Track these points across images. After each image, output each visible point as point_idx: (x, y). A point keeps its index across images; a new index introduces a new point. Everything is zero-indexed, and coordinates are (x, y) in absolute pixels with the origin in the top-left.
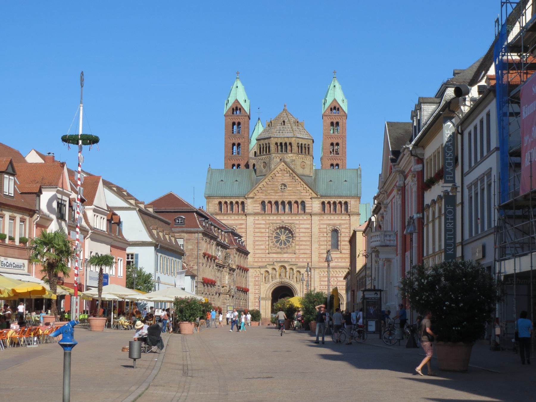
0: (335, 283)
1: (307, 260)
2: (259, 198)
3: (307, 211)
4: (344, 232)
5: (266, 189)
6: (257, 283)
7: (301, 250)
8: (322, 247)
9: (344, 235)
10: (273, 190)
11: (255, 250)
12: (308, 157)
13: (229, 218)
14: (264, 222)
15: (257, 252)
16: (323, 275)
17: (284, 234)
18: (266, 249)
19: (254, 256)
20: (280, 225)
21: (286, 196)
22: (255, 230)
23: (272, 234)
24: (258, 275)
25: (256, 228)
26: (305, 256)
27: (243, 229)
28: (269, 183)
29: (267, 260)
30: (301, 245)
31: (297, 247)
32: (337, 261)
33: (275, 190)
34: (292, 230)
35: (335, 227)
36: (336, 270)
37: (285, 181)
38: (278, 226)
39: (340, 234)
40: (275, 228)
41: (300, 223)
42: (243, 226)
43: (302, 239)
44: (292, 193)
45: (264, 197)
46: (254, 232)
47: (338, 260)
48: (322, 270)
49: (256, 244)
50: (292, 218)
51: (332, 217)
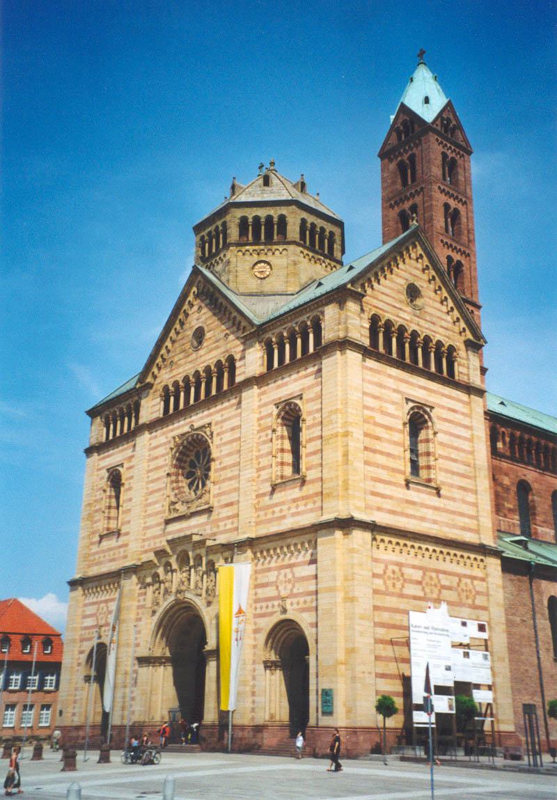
0: (290, 586)
1: (232, 523)
2: (161, 382)
4: (310, 413)
5: (173, 354)
7: (223, 498)
8: (264, 474)
12: (281, 248)
21: (201, 356)
26: (230, 514)
30: (224, 481)
35: (290, 404)
36: (289, 541)
37: (203, 318)
40: (181, 448)
41: (224, 417)
43: (228, 461)
45: (167, 376)
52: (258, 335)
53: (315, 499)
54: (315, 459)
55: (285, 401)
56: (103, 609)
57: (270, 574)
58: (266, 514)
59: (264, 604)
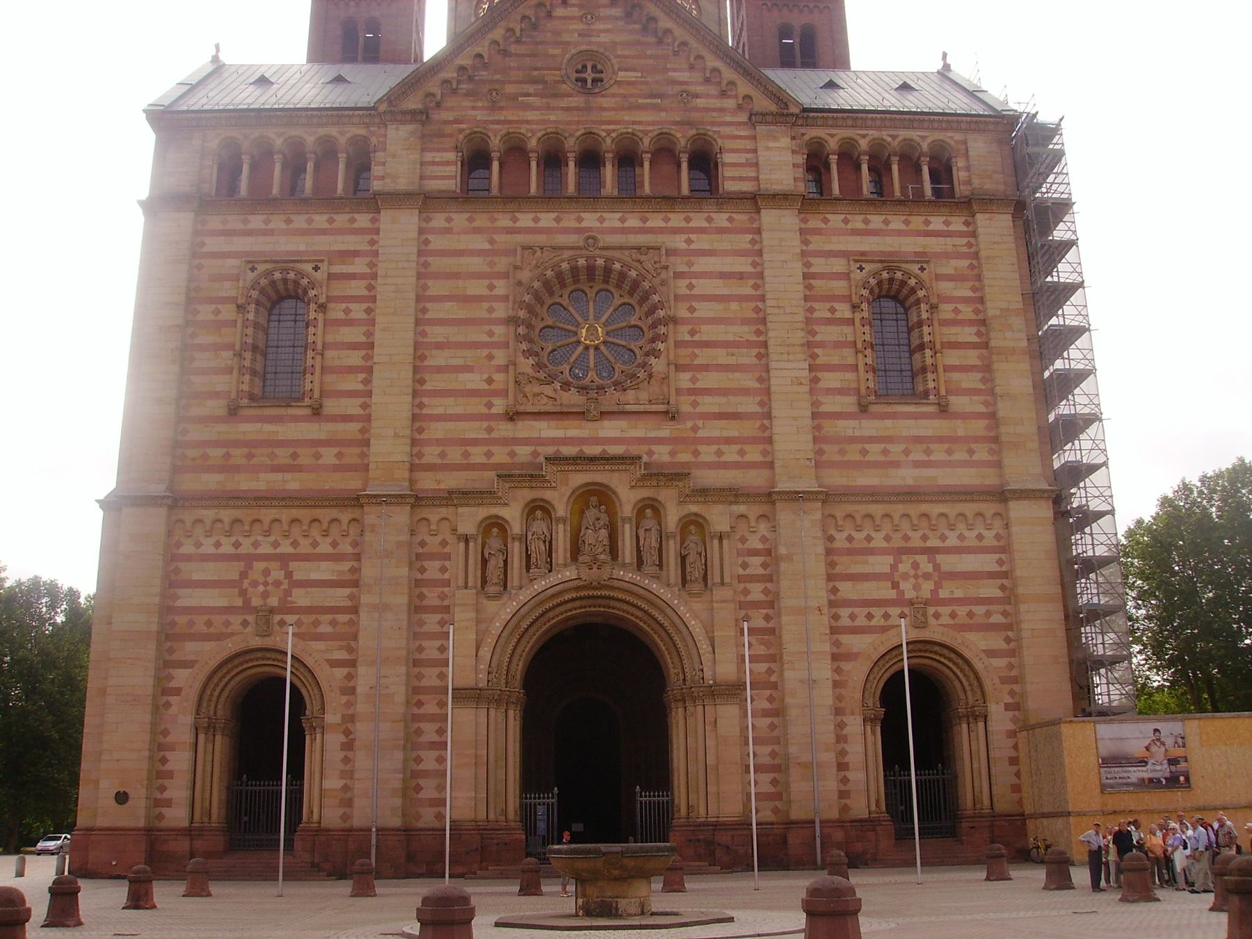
0: (927, 587)
1: (742, 453)
2: (457, 121)
3: (730, 186)
4: (950, 300)
5: (498, 77)
6: (432, 597)
7: (708, 399)
8: (831, 380)
9: (950, 316)
10: (534, 81)
11: (425, 400)
13: (277, 222)
14: (480, 243)
15: (440, 411)
16: (850, 539)
17: (597, 318)
18: (496, 393)
19: (421, 430)
20: (572, 260)
22: (425, 287)
23: (531, 311)
24: (444, 543)
25: (436, 276)
26: (735, 434)
27: (354, 283)
28: (513, 48)
29: (500, 455)
30: (705, 368)
31: (684, 379)
32: (924, 457)
33: (544, 82)
34: (646, 285)
36: (924, 507)
37: (604, 38)
38: (565, 266)
39: (923, 306)
41: (693, 247)
42: (359, 266)
43: (708, 333)
44: (639, 96)
45: (480, 115)
46: (419, 299)
47: (928, 452)
48: (840, 511)
49: (426, 363)
50: (645, 220)
51: (876, 221)
52: (793, 125)
53: (973, 446)
54: (970, 380)
55: (881, 261)
56: (266, 572)
57: (871, 559)
58: (842, 452)
59: (861, 612)
